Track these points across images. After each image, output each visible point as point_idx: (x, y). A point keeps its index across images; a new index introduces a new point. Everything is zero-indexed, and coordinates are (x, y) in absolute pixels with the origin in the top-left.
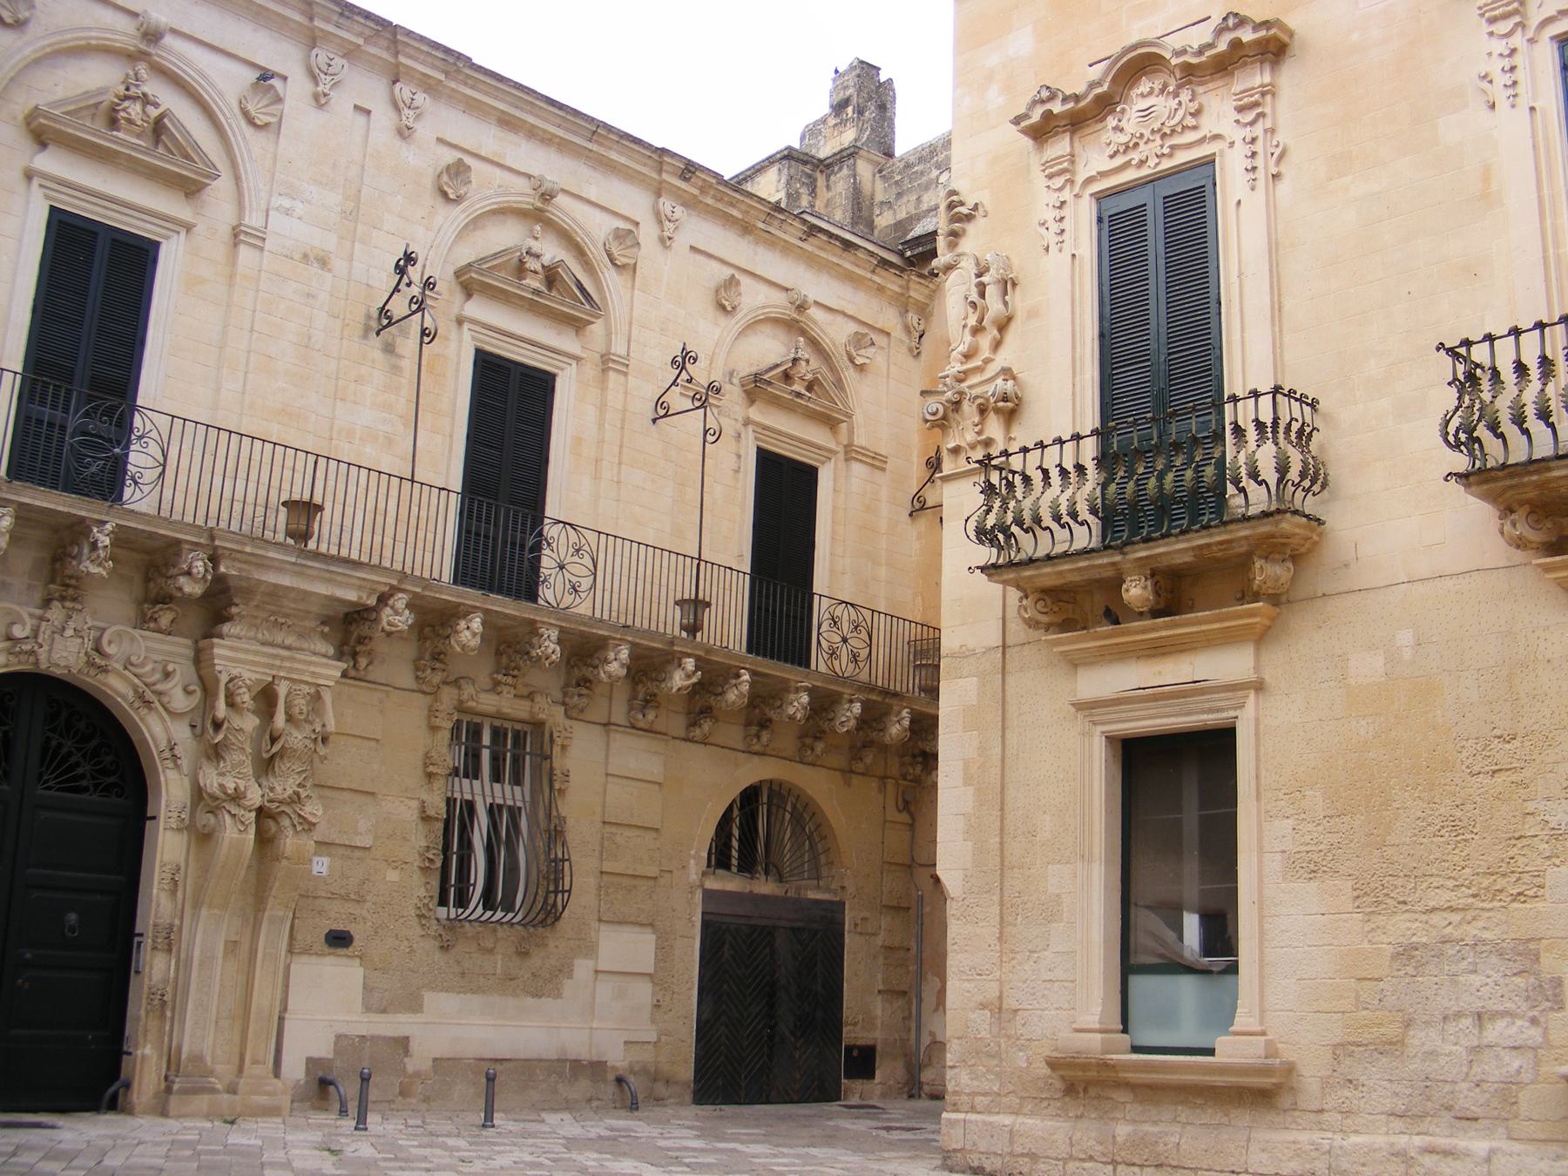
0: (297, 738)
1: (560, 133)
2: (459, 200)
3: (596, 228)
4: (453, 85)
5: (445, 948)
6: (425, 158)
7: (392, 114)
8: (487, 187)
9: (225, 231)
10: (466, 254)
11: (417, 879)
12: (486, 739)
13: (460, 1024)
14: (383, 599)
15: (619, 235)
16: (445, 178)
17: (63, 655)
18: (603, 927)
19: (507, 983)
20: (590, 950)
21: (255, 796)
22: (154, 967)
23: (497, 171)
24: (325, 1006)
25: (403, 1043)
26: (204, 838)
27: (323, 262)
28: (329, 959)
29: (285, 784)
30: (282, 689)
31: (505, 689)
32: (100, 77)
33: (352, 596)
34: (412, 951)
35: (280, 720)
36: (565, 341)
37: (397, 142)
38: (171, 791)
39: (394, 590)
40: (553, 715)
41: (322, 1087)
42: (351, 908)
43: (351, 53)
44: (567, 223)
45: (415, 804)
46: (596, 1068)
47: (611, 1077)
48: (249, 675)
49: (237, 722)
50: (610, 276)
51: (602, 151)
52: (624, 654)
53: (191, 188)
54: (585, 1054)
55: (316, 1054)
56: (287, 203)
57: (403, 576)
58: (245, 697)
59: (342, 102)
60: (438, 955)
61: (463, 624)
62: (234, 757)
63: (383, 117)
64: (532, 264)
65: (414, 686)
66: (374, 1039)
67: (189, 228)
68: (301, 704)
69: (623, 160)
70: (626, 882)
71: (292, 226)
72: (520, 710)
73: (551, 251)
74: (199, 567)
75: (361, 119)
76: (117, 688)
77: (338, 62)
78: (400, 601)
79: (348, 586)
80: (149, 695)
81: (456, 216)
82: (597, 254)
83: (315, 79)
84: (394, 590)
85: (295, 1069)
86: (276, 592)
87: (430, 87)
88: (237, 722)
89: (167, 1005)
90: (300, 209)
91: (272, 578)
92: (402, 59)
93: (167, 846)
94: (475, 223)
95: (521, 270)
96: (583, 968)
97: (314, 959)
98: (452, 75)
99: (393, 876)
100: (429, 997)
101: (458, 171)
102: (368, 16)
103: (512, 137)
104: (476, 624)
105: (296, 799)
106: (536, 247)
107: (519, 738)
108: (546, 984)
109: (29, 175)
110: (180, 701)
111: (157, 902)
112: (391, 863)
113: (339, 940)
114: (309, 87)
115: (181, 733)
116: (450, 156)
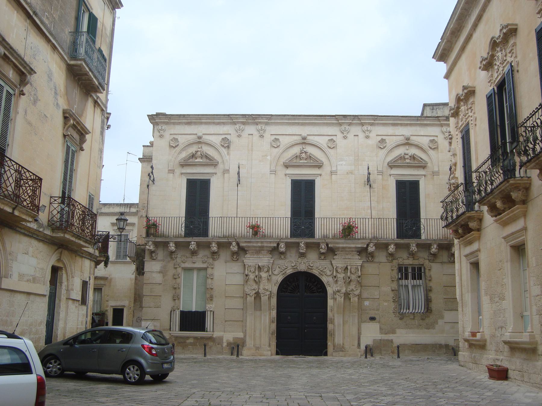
0: (353, 277)
1: (409, 122)
2: (384, 147)
3: (424, 141)
4: (377, 122)
5: (401, 319)
6: (374, 140)
7: (364, 134)
8: (391, 142)
9: (329, 172)
10: (389, 159)
11: (392, 304)
12: (410, 270)
13: (404, 336)
14: (368, 245)
15: (432, 141)
16: (379, 144)
17: (302, 267)
18: (446, 312)
19: (419, 326)
20: (442, 317)
21: (343, 290)
22: (330, 327)
23: (394, 137)
24: (371, 334)
25: (392, 341)
26: (335, 299)
27: (352, 173)
28: (371, 323)
29: (352, 286)
30: (349, 268)
31: (410, 258)
32: (296, 150)
33: (359, 246)
34: (393, 320)
35: (349, 274)
36: (421, 172)
37: (366, 140)
38: (330, 291)
39: (370, 243)
40: (427, 263)
41: (369, 351)
42: (377, 312)
43: (350, 124)
44: (416, 143)
45: (390, 287)
46: (447, 346)
47: (450, 348)
48: (340, 265)
49: (339, 275)
50: (431, 152)
51: (422, 122)
52: (435, 246)
53: (319, 166)
54: (443, 343)
55: (368, 344)
56: (341, 163)
57: (371, 240)
58: (339, 270)
59: (351, 136)
60: (399, 320)
61: (390, 247)
62: (339, 283)
63: (361, 135)
64: (406, 157)
65: (386, 261)
66: (384, 340)
67: (320, 175)
68: (353, 270)
69: (428, 122)
70: (451, 300)
71: (343, 167)
72: (416, 262)
73: (413, 151)
74: (323, 247)
75: (356, 137)
76: (315, 272)
77: (347, 127)
78: (371, 245)
79: (358, 244)
80: (321, 273)
81: (385, 151)
82: (426, 147)
83: (343, 133)
84: (370, 243)
85: (363, 347)
86: (343, 248)
87: (372, 124)
88: (339, 275)
89: (333, 335)
90: (344, 163)
91: (341, 246)
92: (362, 121)
93: (330, 302)
94: (391, 150)
95: (405, 159)
96: (440, 322)
97: (367, 323)
98: (376, 120)
99: (386, 304)
100: (398, 331)
101: (383, 141)
102: (350, 116)
103: (397, 127)
104: (392, 246)
105: (352, 290)
106: (407, 152)
107: (420, 268)
108: (430, 326)
109: (286, 175)
110: (329, 273)
111: (330, 314)
112: (386, 301)
113: (372, 319)
114: (342, 135)
115: (331, 279)
116: (379, 138)
